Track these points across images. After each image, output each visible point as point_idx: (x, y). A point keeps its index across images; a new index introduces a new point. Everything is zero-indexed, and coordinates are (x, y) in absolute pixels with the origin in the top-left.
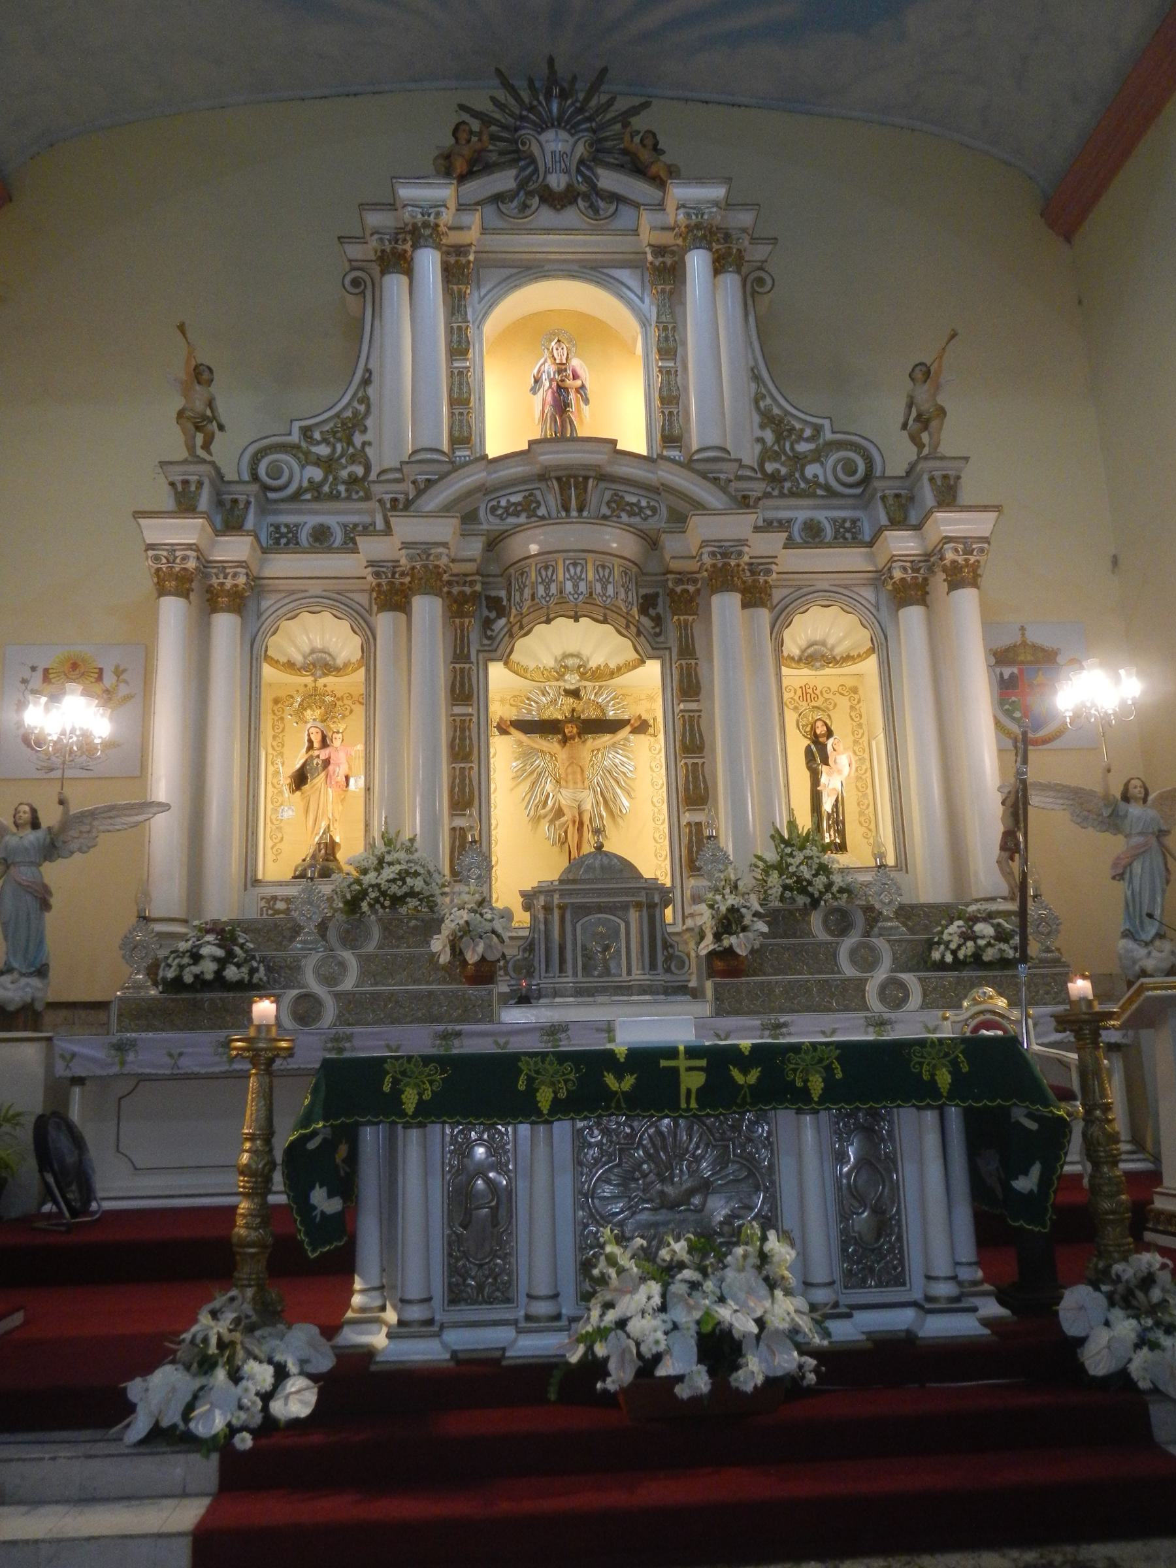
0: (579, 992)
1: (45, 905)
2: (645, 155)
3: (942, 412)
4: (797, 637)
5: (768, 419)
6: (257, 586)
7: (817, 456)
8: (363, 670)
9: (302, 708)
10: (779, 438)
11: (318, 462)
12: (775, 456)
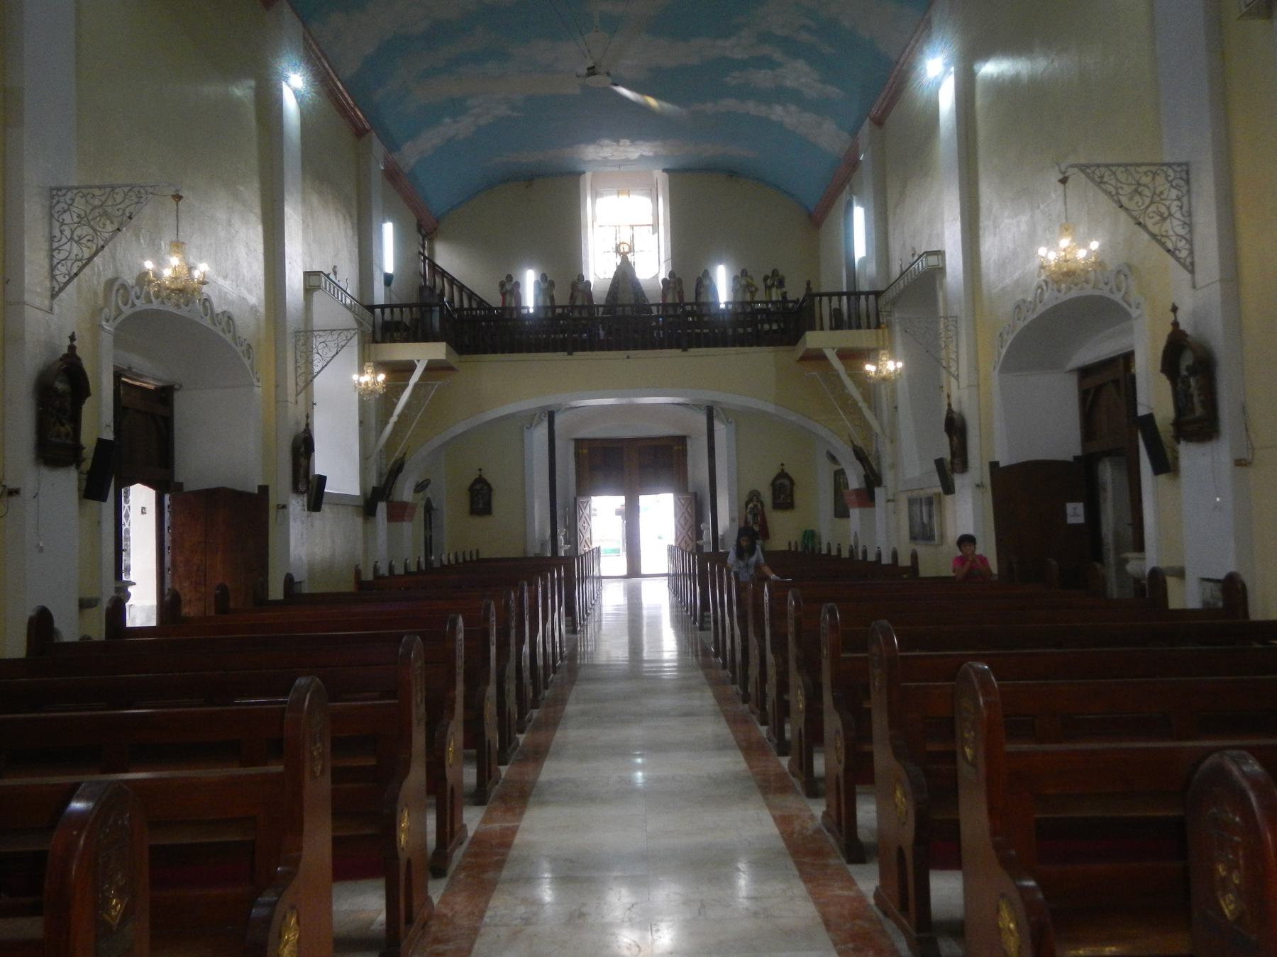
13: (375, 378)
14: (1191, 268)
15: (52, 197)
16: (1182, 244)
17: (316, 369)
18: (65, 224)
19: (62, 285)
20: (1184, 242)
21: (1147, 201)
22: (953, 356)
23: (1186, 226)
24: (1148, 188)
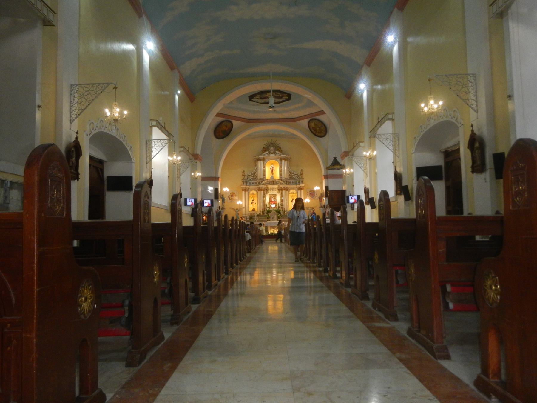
0: (272, 220)
1: (239, 214)
2: (280, 149)
3: (303, 174)
4: (291, 192)
5: (290, 172)
6: (249, 188)
7: (294, 175)
8: (256, 195)
9: (252, 197)
10: (291, 174)
11: (252, 176)
12: (290, 175)
13: (177, 158)
14: (477, 111)
15: (71, 88)
16: (474, 102)
17: (154, 154)
18: (76, 97)
19: (74, 119)
20: (474, 102)
21: (461, 87)
22: (397, 149)
23: (475, 96)
24: (461, 82)
